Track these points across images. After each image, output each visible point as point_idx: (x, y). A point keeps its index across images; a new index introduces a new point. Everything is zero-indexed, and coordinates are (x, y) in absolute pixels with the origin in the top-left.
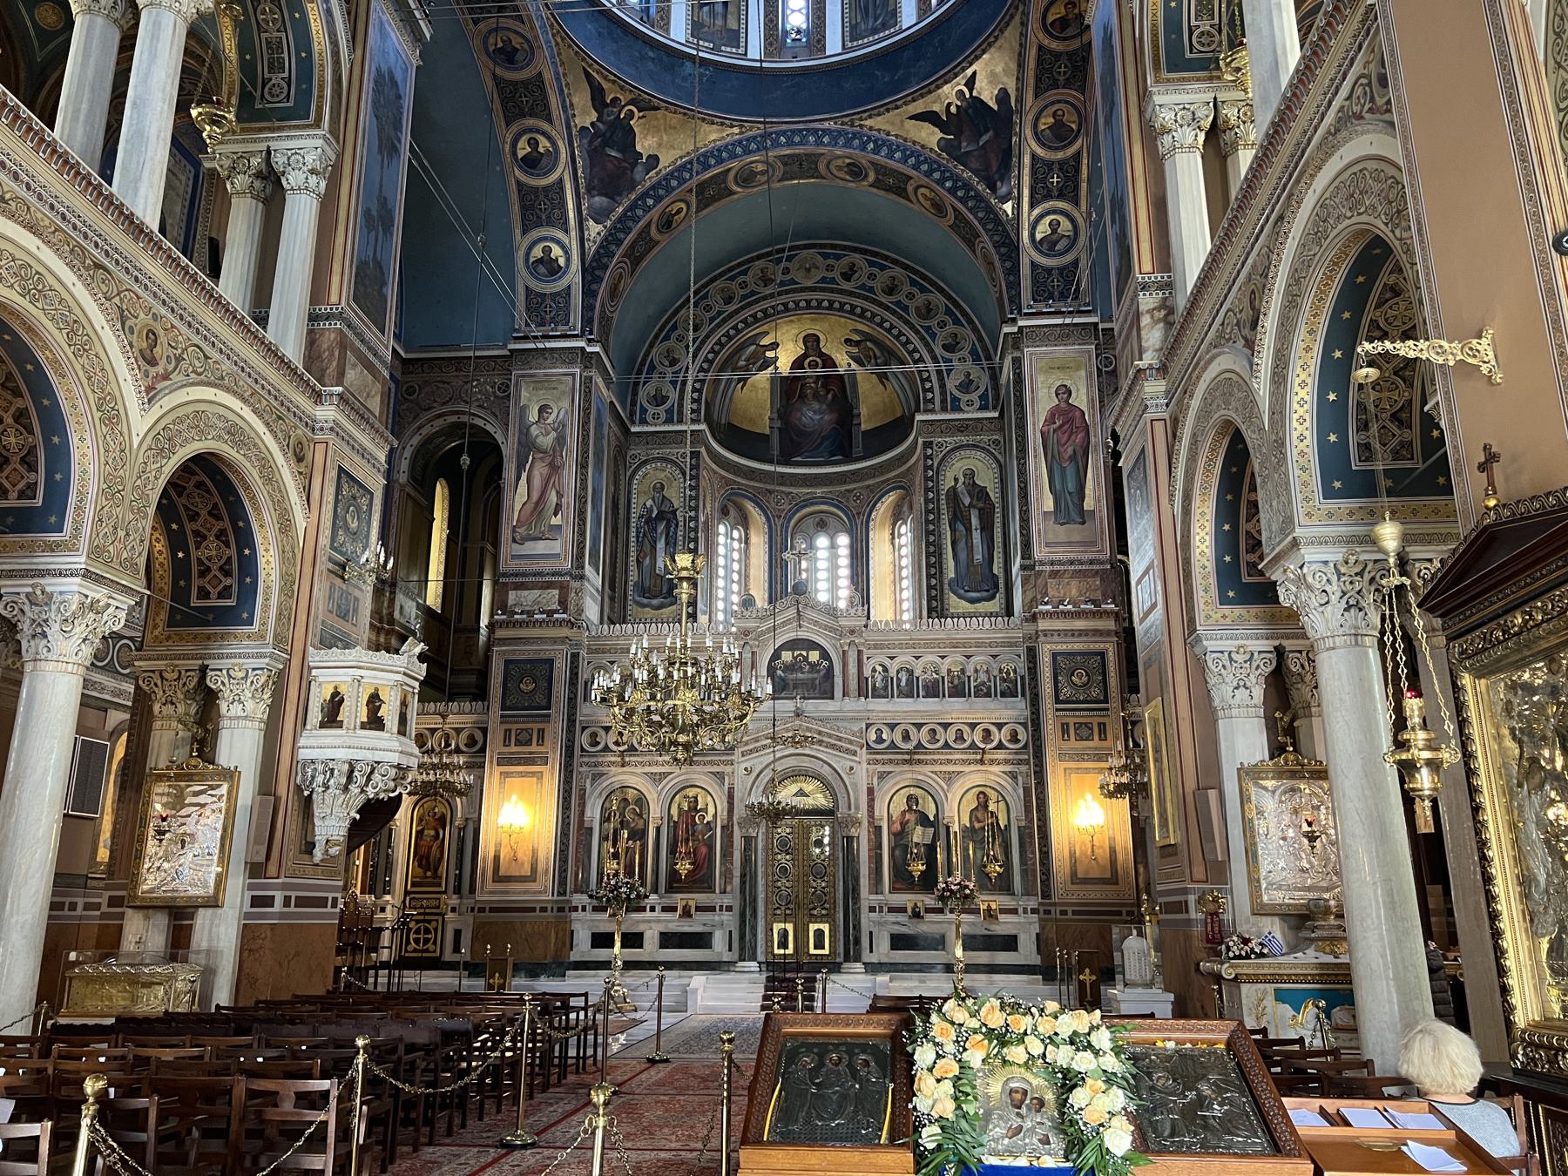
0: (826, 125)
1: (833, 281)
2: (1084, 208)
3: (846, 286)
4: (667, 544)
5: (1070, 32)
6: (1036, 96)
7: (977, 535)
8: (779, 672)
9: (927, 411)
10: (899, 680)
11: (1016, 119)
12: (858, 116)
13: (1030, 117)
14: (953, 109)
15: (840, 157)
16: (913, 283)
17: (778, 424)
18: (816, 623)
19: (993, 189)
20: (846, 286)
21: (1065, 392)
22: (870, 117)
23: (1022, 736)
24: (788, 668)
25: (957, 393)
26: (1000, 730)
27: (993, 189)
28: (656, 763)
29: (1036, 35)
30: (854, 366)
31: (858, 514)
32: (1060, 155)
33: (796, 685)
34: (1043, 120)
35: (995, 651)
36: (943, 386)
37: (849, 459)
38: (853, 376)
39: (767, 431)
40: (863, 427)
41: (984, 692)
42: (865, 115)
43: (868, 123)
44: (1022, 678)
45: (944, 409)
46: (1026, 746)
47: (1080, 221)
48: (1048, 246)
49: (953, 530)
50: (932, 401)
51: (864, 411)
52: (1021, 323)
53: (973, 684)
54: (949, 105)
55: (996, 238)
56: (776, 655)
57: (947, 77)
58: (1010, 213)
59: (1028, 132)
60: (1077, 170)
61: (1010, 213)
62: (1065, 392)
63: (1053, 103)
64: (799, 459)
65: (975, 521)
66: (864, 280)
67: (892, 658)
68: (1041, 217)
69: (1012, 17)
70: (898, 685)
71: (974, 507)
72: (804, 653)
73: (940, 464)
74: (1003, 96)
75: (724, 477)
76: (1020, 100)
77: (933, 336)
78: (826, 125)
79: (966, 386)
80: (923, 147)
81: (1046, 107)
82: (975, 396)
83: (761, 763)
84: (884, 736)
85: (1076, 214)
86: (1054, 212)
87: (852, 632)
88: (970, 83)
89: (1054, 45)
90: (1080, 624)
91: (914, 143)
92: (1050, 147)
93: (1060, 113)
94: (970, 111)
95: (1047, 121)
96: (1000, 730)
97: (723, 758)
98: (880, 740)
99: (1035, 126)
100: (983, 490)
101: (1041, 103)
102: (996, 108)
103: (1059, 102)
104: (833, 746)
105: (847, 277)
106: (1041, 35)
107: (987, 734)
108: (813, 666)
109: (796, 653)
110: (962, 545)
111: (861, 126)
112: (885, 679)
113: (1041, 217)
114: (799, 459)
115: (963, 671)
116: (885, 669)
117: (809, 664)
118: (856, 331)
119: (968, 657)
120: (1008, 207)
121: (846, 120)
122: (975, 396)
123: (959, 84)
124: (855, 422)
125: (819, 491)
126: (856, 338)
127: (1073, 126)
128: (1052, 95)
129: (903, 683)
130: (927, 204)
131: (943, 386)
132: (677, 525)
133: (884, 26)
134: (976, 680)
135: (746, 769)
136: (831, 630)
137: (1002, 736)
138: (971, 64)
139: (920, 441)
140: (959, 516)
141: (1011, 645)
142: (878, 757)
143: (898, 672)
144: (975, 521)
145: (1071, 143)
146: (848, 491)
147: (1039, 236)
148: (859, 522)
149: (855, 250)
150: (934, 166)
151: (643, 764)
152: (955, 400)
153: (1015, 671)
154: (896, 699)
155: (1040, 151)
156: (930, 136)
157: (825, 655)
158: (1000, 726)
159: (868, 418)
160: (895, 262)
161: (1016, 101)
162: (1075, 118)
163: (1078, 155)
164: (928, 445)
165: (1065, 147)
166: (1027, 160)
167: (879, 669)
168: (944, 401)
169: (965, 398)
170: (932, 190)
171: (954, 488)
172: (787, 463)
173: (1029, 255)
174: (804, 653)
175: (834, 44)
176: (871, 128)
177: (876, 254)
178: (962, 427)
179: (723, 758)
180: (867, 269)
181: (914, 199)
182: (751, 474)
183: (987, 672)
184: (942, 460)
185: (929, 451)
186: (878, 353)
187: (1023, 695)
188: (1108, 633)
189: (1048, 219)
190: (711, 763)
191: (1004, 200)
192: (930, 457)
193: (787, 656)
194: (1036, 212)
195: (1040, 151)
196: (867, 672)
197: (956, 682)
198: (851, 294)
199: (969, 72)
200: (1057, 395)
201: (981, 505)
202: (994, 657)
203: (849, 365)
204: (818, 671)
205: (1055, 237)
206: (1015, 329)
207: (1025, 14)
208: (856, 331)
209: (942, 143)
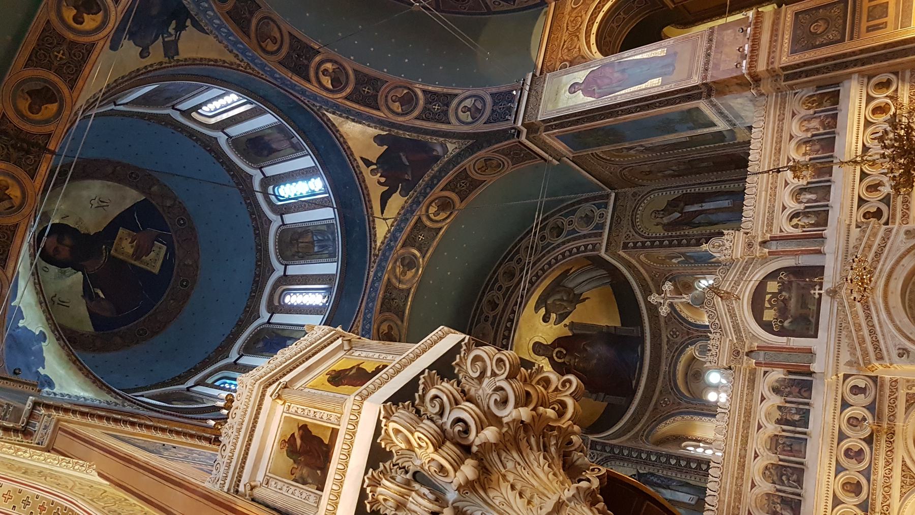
0: (372, 274)
1: (495, 317)
2: (460, 91)
3: (501, 307)
4: (667, 487)
5: (343, 79)
6: (378, 109)
7: (707, 206)
8: (786, 324)
9: (599, 250)
10: (809, 201)
11: (394, 131)
12: (373, 250)
13: (390, 115)
14: (383, 180)
15: (394, 268)
16: (511, 259)
17: (602, 395)
18: (737, 283)
19: (437, 158)
20: (501, 307)
21: (573, 88)
22: (375, 242)
23: (883, 78)
24: (783, 312)
25: (592, 226)
26: (874, 99)
27: (437, 158)
28: (888, 477)
29: (339, 98)
30: (567, 321)
31: (688, 333)
32: (421, 102)
33: (804, 300)
34: (395, 109)
35: (788, 115)
36: (585, 236)
37: (642, 340)
38: (572, 326)
39: (605, 404)
40: (618, 324)
41: (832, 121)
42: (373, 245)
43: (378, 244)
44: (819, 88)
45: (601, 235)
46: (896, 74)
47: (468, 93)
48: (476, 113)
49: (699, 225)
50: (594, 245)
51: (603, 322)
52: (519, 124)
53: (822, 131)
54: (379, 182)
55: (467, 155)
56: (767, 327)
57: (361, 180)
58: (454, 146)
59: (400, 119)
60: (435, 93)
61: (454, 146)
62: (573, 88)
63: (386, 101)
64: (634, 382)
65: (695, 208)
66: (500, 294)
67: (784, 208)
68: (457, 118)
69: (329, 120)
70: (816, 201)
71: (683, 209)
72: (768, 297)
73: (642, 236)
74: (379, 139)
75: (629, 439)
76: (380, 123)
77: (549, 244)
78: (372, 274)
79: (588, 219)
80: (403, 208)
81: (387, 105)
82: (597, 212)
83: (893, 337)
84: (874, 210)
85: (462, 96)
86: (457, 109)
87: (750, 245)
88: (368, 163)
89: (348, 90)
90: (765, 37)
91: (399, 214)
92: (415, 108)
93: (394, 98)
94: (386, 168)
95: (396, 106)
96: (874, 99)
97: (887, 392)
98: (878, 214)
99: (398, 114)
100: (670, 204)
101: (384, 108)
102: (386, 147)
103: (386, 96)
104: (878, 255)
105: (494, 305)
106: (339, 96)
107: (878, 110)
108: (784, 287)
109: (767, 305)
110: (713, 218)
111: (379, 250)
112: (806, 214)
113: (457, 118)
114: (634, 382)
115: (806, 142)
116: (796, 215)
117: (780, 291)
118: (537, 309)
119: (791, 137)
120: (451, 147)
121: (373, 259)
122: (597, 212)
123: (366, 171)
124: (613, 332)
125: (664, 368)
126: (543, 311)
127: (405, 92)
128: (381, 101)
129: (813, 197)
130: (443, 215)
131: (585, 236)
132: (653, 474)
133: (333, 233)
134: (818, 129)
135: (900, 356)
136: (745, 268)
137: (881, 98)
138: (355, 160)
139: (621, 253)
140: (689, 221)
141: (783, 103)
142: (899, 215)
143: (801, 202)
144: (695, 208)
145: (416, 95)
146: (668, 342)
147: (470, 120)
148: (696, 334)
149: (481, 300)
150: (416, 202)
151: (887, 496)
152: (596, 227)
153: (811, 96)
154: (830, 203)
155: (416, 113)
156: (397, 202)
157: (773, 275)
158: (870, 99)
159: (608, 319)
160: (495, 273)
161: (382, 130)
162: (400, 90)
163: (424, 91)
164: (625, 246)
165: (417, 98)
166: (418, 123)
167: (795, 221)
168: (595, 235)
169: (597, 220)
170: (430, 204)
171: (664, 225)
172: (634, 392)
173: (480, 127)
174: (768, 297)
175: (330, 268)
176: (383, 243)
177: (487, 285)
178: (616, 221)
179: (887, 392)
180: (494, 293)
181: (439, 225)
182: (634, 421)
183: (809, 119)
184: (639, 234)
185: (631, 244)
186: (558, 297)
187: (837, 84)
188: (777, 13)
189: (460, 113)
190: (892, 408)
191: (446, 150)
192: (635, 244)
193: (769, 315)
194: (453, 119)
195: (416, 113)
196: (798, 231)
197: (817, 147)
198: (506, 304)
199: (361, 163)
200: (574, 92)
201: (682, 204)
202: (794, 115)
203: (565, 325)
204: (790, 282)
205: (473, 110)
206: (525, 130)
207: (326, 102)
208: (537, 309)
209: (403, 192)
